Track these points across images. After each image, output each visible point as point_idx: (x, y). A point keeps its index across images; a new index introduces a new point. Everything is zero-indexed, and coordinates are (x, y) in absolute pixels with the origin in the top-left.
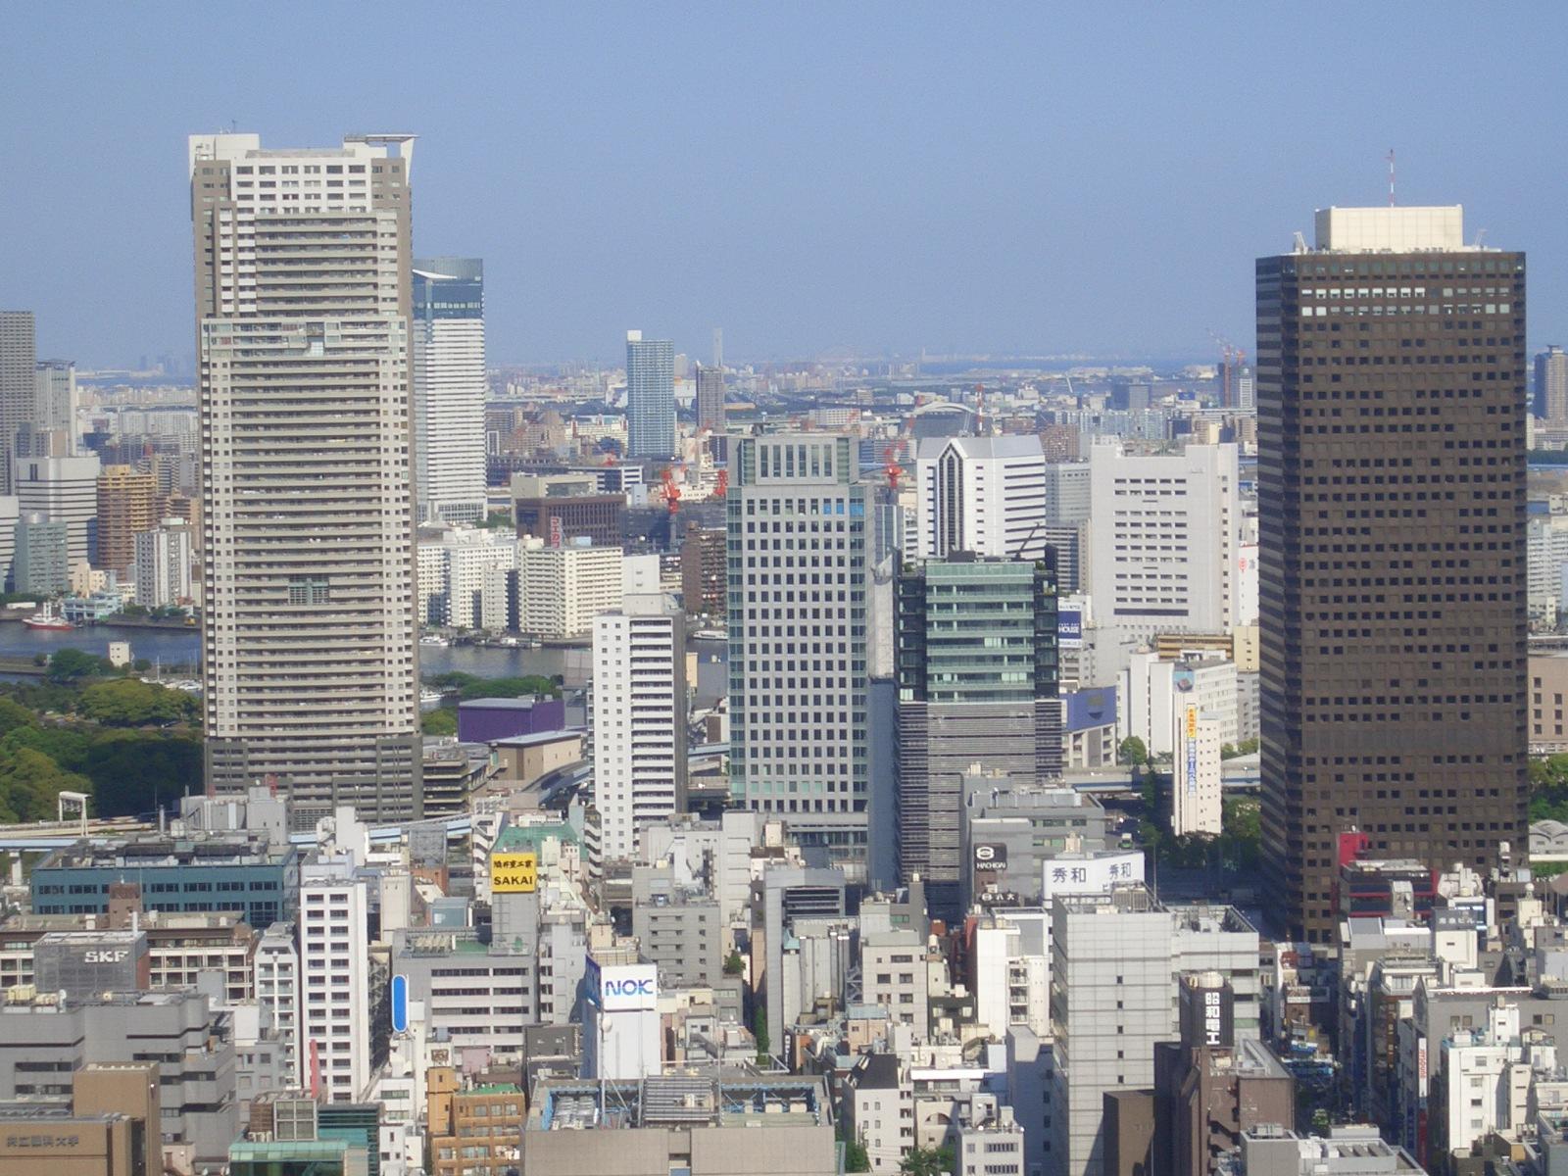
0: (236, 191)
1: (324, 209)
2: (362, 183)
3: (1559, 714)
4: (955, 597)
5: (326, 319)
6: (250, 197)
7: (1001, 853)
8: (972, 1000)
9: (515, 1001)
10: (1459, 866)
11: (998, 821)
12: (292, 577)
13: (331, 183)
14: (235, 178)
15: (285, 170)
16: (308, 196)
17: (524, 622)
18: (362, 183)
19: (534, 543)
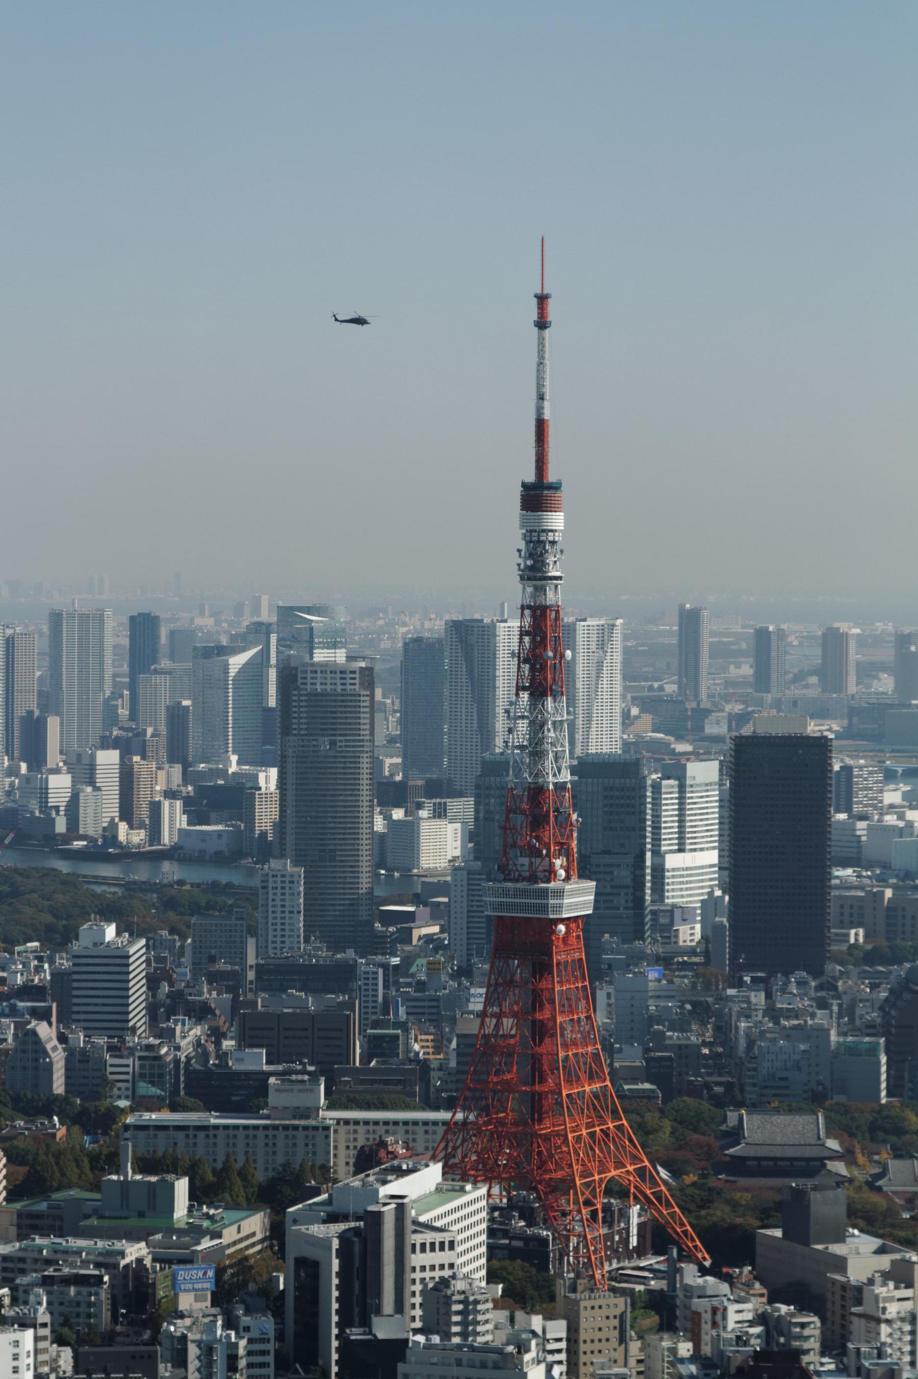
0: (300, 681)
1: (339, 690)
2: (354, 678)
3: (913, 926)
4: (602, 869)
5: (339, 738)
6: (305, 684)
7: (610, 967)
10: (779, 975)
12: (321, 851)
13: (341, 678)
14: (300, 675)
15: (322, 672)
16: (331, 684)
17: (389, 862)
18: (354, 678)
19: (398, 814)
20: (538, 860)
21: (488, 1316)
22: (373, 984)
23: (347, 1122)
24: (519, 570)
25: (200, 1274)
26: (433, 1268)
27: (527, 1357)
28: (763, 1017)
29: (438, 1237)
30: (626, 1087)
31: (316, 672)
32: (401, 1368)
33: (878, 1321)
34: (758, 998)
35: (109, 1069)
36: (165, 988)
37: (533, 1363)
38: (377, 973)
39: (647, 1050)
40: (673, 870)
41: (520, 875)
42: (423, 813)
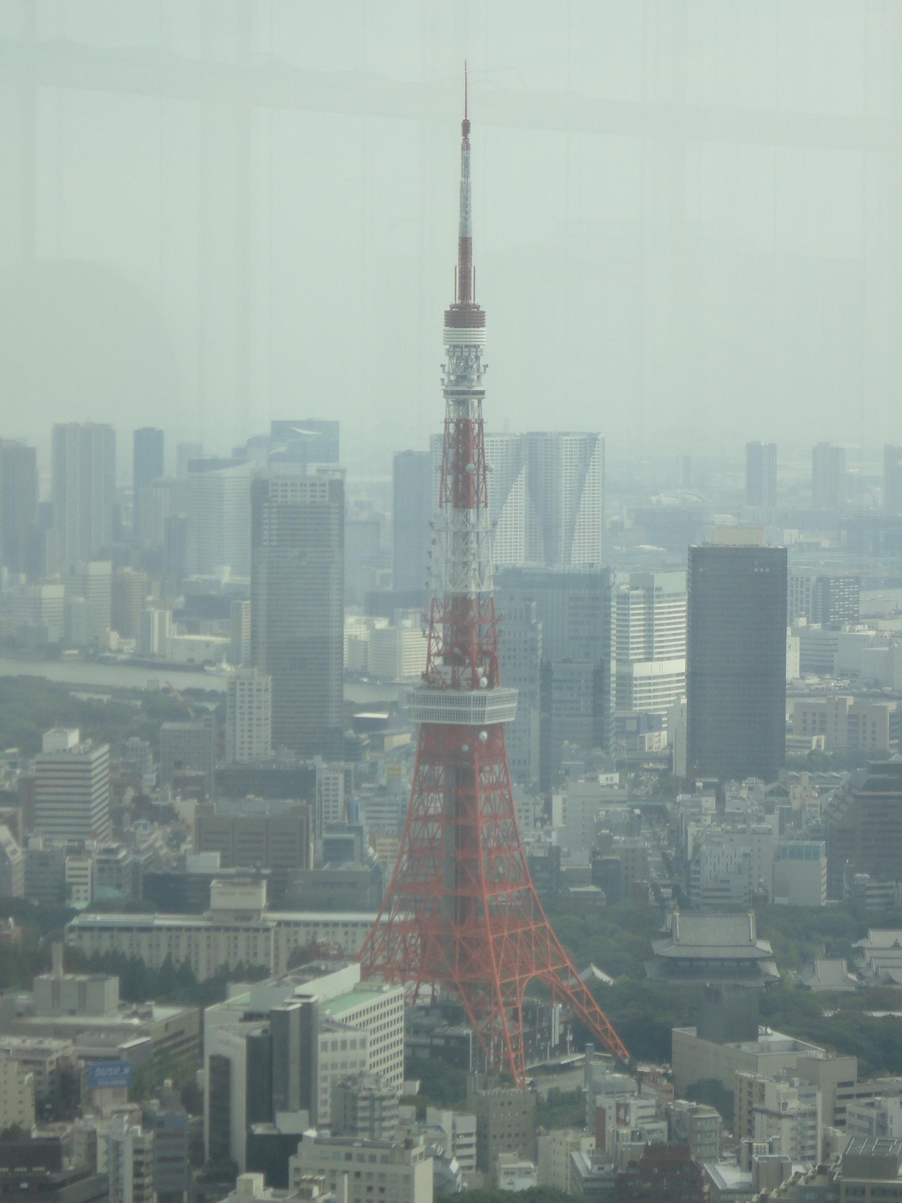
2: (324, 491)
6: (277, 496)
8: (550, 818)
9: (394, 815)
11: (572, 763)
19: (381, 624)
20: (461, 669)
21: (394, 1112)
22: (334, 790)
23: (288, 924)
24: (443, 384)
25: (117, 1071)
26: (344, 1065)
27: (415, 1152)
28: (712, 821)
29: (350, 1035)
30: (572, 890)
31: (286, 485)
32: (293, 1162)
33: (780, 1116)
34: (709, 802)
35: (68, 873)
36: (130, 793)
37: (421, 1158)
38: (336, 779)
39: (594, 853)
40: (641, 678)
41: (444, 683)
42: (407, 623)
